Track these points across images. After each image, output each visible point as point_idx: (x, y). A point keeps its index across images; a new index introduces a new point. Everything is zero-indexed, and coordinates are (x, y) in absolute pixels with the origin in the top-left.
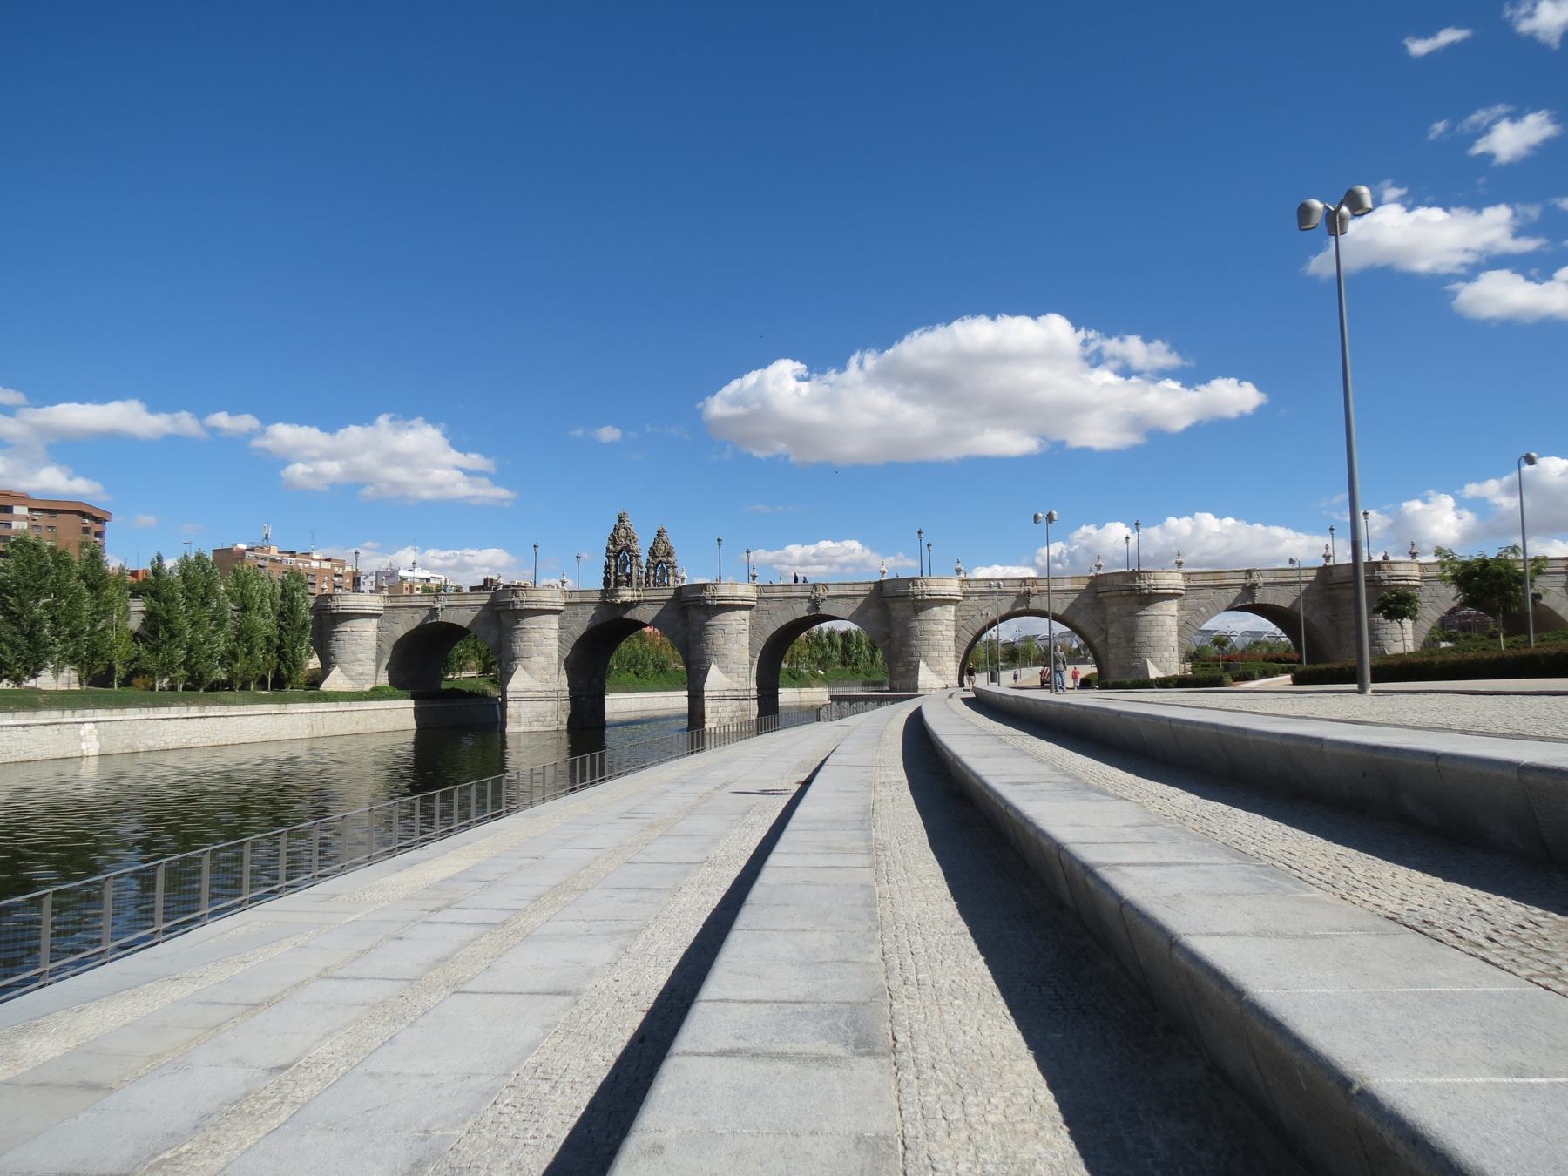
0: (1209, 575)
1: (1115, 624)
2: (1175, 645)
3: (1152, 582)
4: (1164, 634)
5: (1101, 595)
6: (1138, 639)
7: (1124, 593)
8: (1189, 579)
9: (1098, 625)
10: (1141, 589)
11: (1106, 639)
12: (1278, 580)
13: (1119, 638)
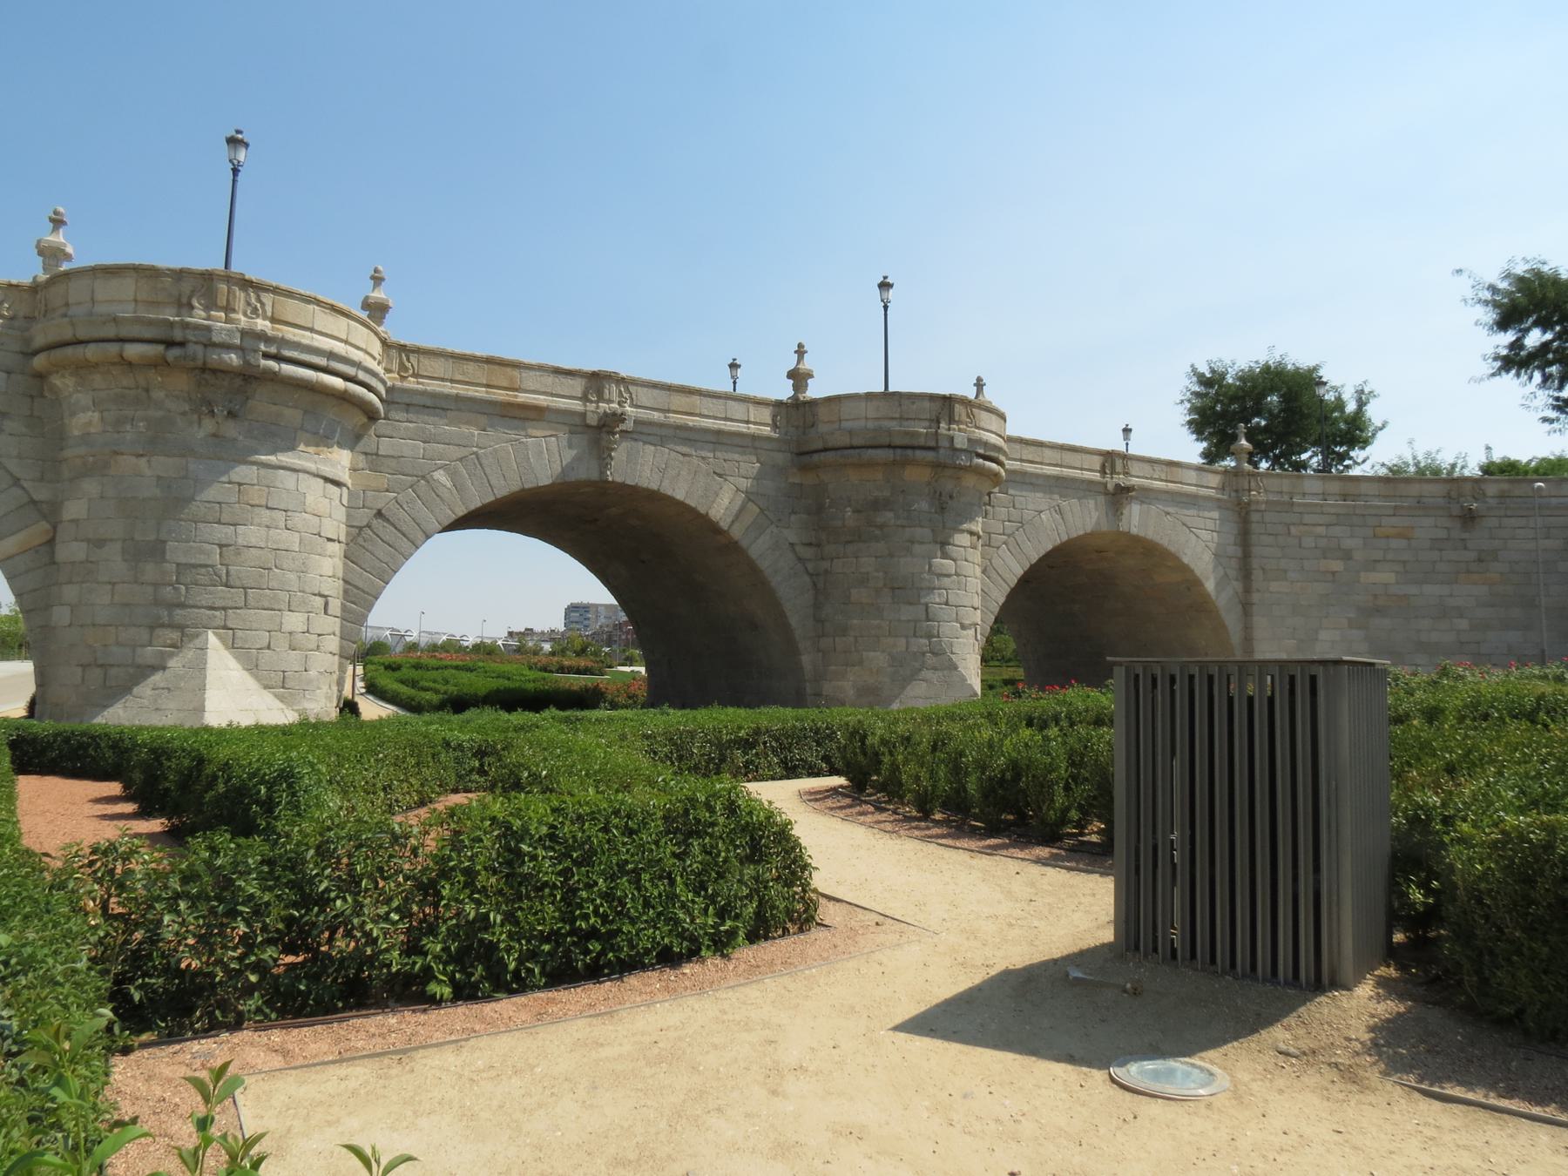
0: (471, 367)
1: (91, 486)
2: (334, 588)
3: (262, 324)
4: (293, 540)
5: (39, 362)
6: (176, 552)
7: (133, 351)
8: (402, 367)
9: (16, 482)
10: (210, 345)
11: (51, 542)
12: (675, 418)
13: (100, 543)
